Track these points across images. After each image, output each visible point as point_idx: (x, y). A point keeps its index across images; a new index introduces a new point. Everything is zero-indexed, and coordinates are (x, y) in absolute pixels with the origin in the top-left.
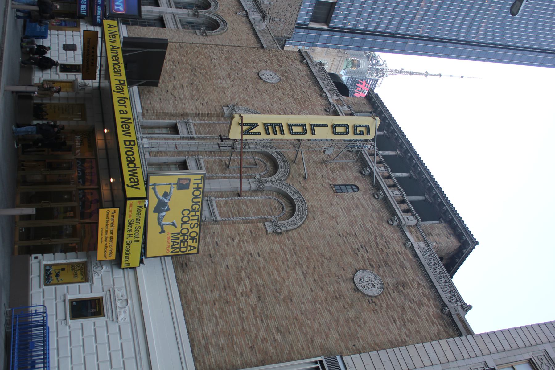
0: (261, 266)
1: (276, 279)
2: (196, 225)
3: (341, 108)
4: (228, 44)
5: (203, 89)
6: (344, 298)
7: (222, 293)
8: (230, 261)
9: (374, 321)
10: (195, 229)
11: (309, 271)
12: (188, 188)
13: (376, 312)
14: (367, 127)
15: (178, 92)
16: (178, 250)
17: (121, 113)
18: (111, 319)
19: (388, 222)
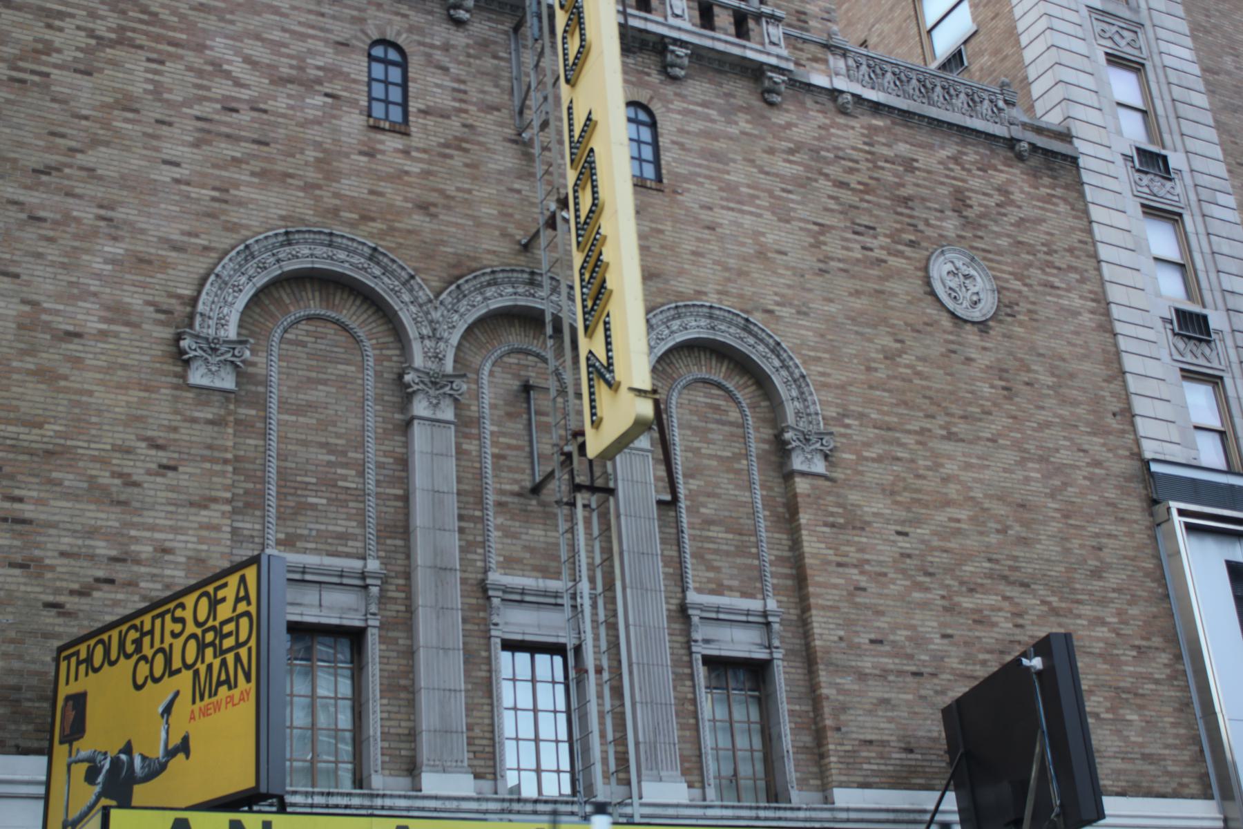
5: (40, 426)
8: (929, 624)
15: (63, 554)
19: (771, 104)
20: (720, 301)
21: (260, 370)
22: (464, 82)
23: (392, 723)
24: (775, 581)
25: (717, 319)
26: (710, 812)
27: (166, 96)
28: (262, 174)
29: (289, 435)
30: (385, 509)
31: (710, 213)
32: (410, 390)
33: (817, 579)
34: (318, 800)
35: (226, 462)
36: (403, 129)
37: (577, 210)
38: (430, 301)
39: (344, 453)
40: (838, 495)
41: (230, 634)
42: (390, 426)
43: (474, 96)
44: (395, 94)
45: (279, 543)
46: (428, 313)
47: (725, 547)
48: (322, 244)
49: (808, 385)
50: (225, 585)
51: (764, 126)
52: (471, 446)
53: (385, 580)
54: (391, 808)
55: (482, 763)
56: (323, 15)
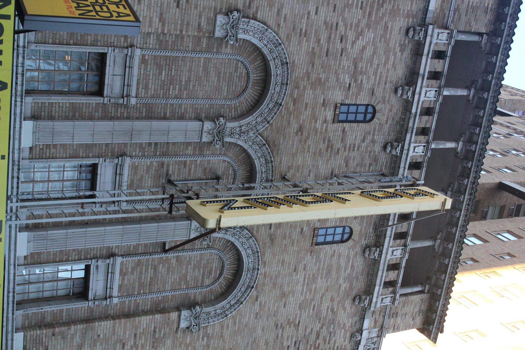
3: (434, 41)
19: (354, 300)
20: (261, 274)
21: (224, 50)
22: (358, 150)
23: (57, 108)
24: (127, 303)
25: (253, 272)
26: (12, 267)
27: (347, 9)
28: (313, 53)
29: (194, 63)
30: (160, 108)
31: (302, 269)
32: (216, 120)
33: (128, 323)
34: (20, 69)
35: (181, 31)
36: (336, 120)
37: (303, 196)
38: (257, 131)
39: (186, 89)
40: (169, 334)
41: (102, 9)
42: (198, 112)
43: (352, 154)
44: (351, 117)
45: (144, 56)
46: (252, 130)
47: (143, 277)
48: (282, 80)
49: (222, 318)
50: (125, 8)
51: (344, 296)
52: (190, 151)
53: (126, 106)
54: (15, 105)
55: (38, 153)
56: (385, 83)
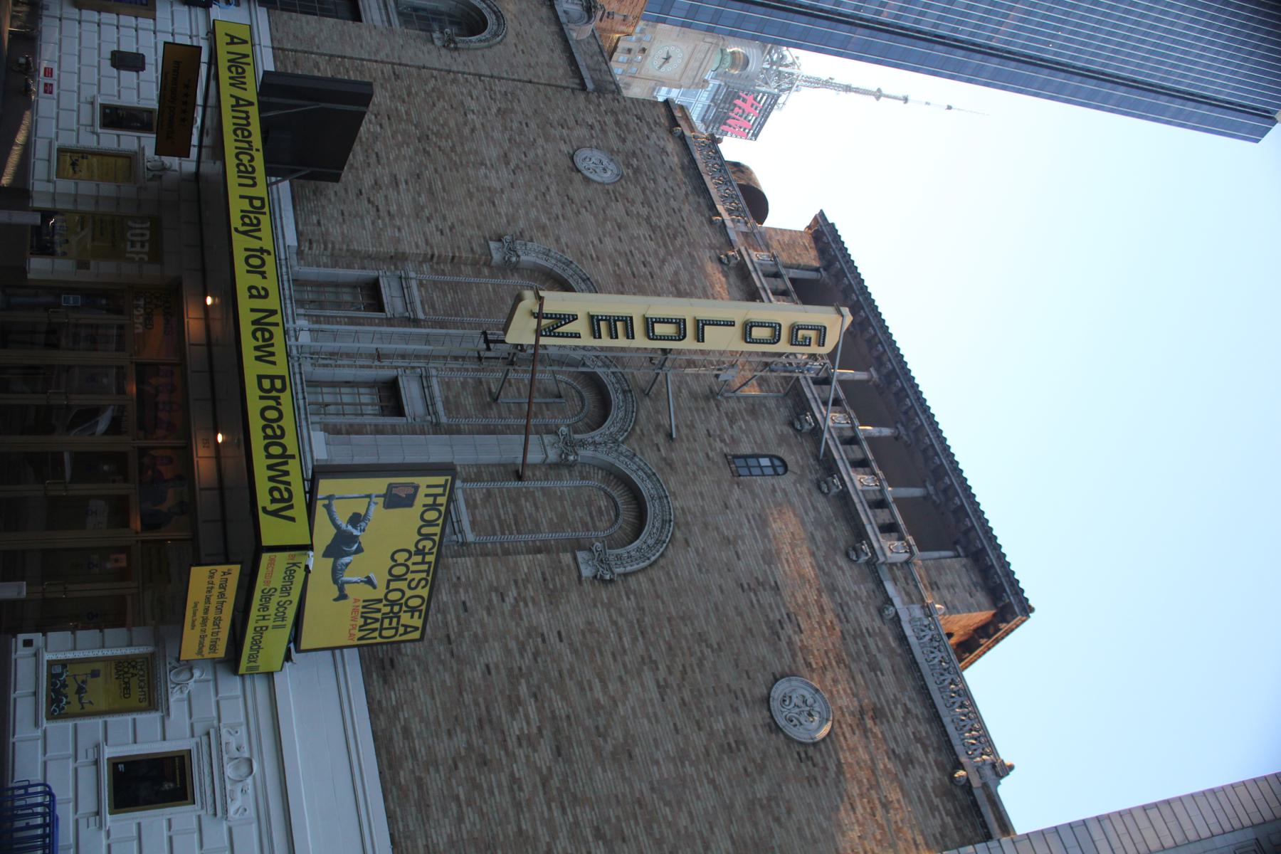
0: (566, 666)
1: (598, 701)
2: (423, 583)
3: (755, 260)
4: (505, 75)
6: (747, 749)
7: (474, 737)
8: (494, 653)
9: (809, 805)
10: (419, 591)
11: (671, 680)
12: (410, 505)
13: (813, 783)
14: (821, 331)
15: (386, 197)
16: (376, 634)
17: (252, 296)
18: (211, 812)
19: (847, 555)
